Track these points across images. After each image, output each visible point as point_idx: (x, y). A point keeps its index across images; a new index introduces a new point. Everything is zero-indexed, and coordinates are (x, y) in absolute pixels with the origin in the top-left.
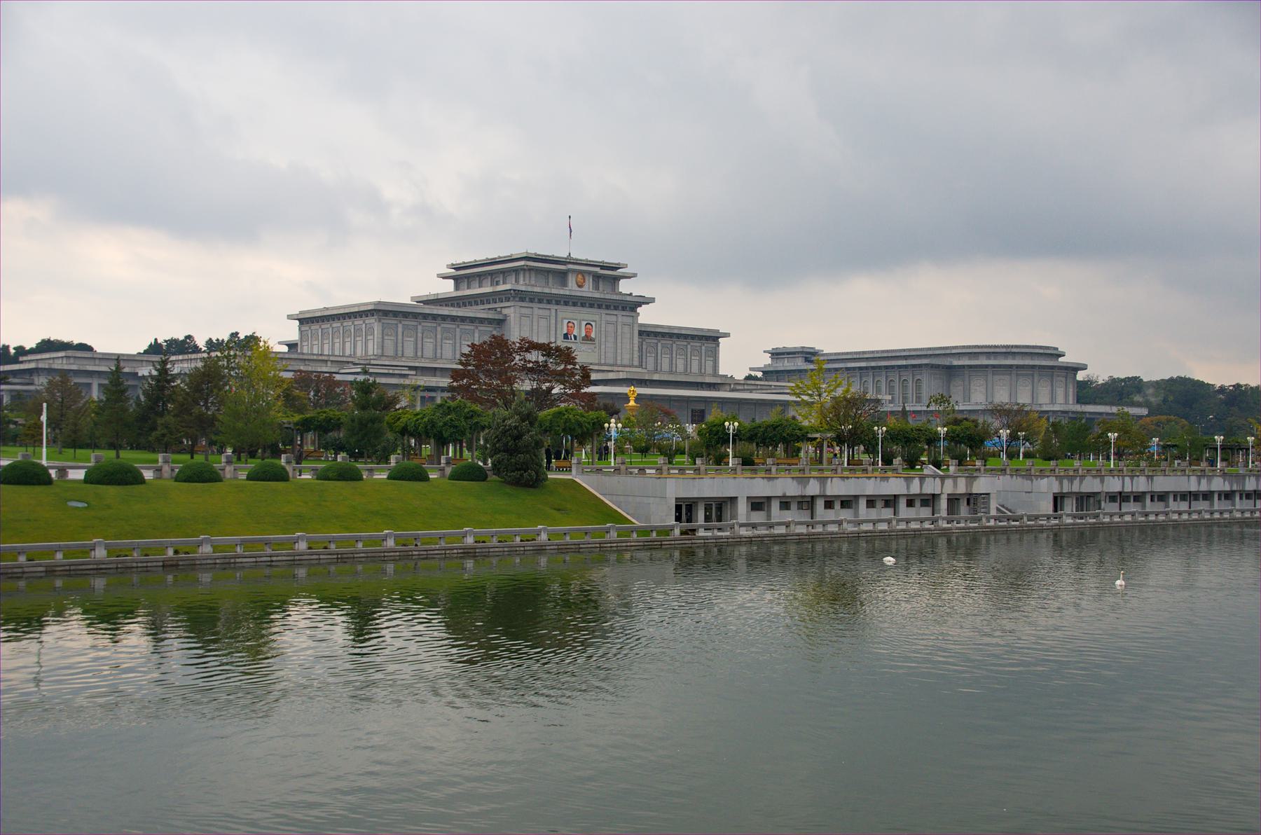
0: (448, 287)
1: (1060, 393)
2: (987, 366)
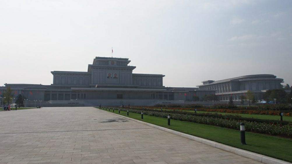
2: (249, 81)
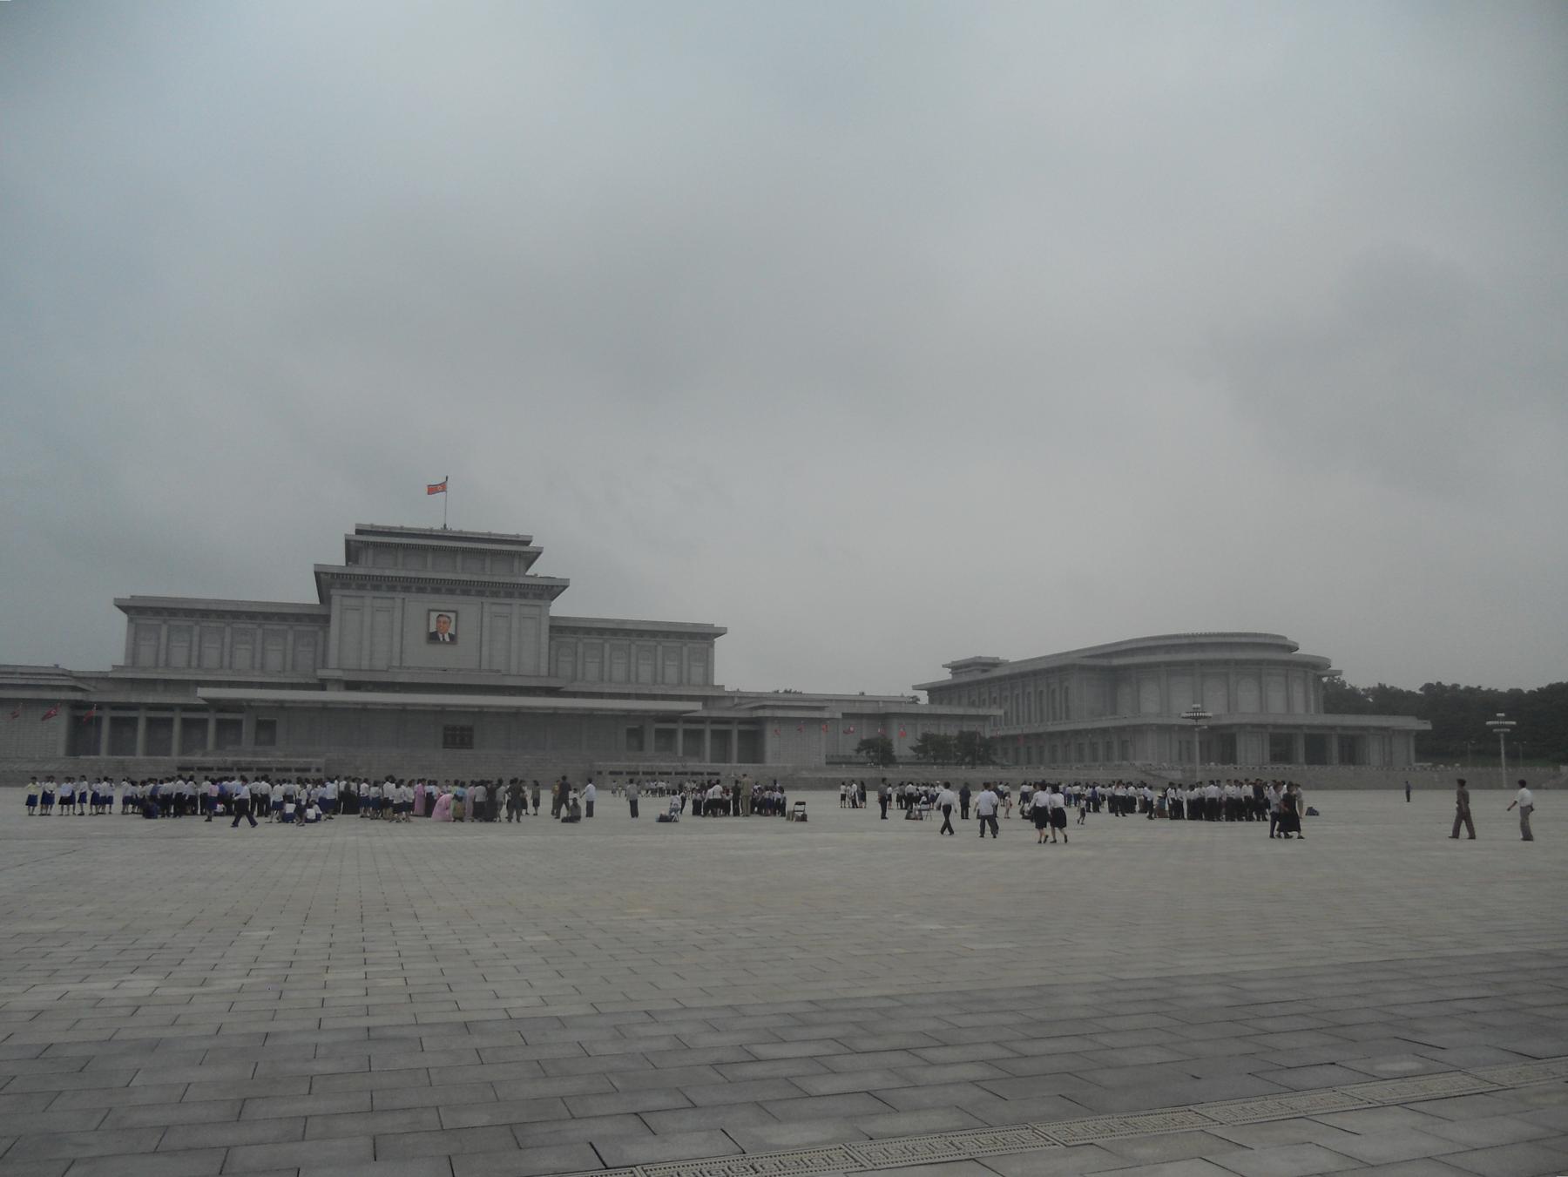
1: (1298, 693)
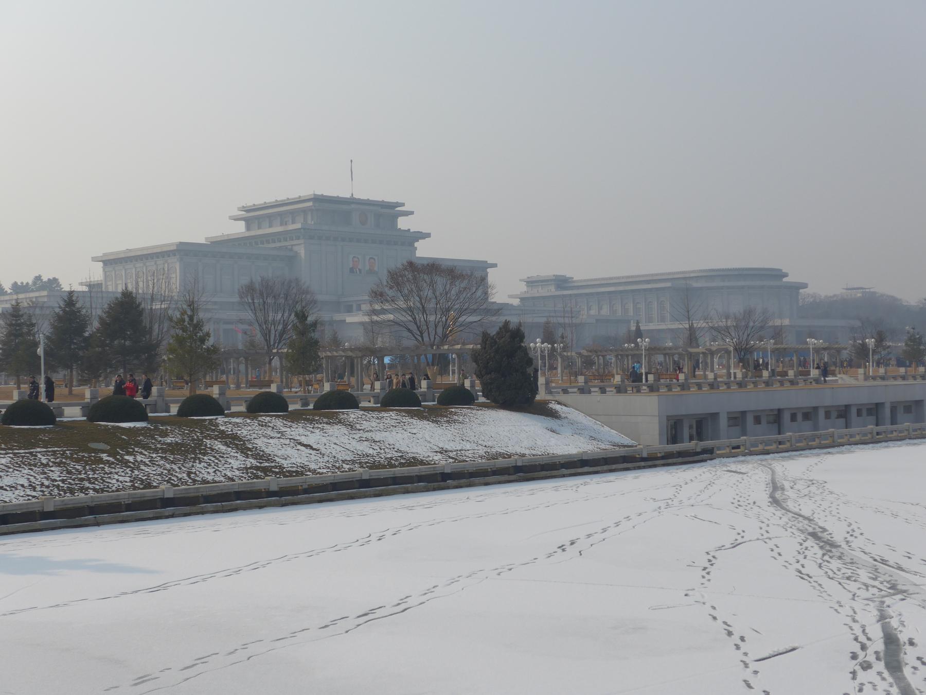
0: (239, 228)
